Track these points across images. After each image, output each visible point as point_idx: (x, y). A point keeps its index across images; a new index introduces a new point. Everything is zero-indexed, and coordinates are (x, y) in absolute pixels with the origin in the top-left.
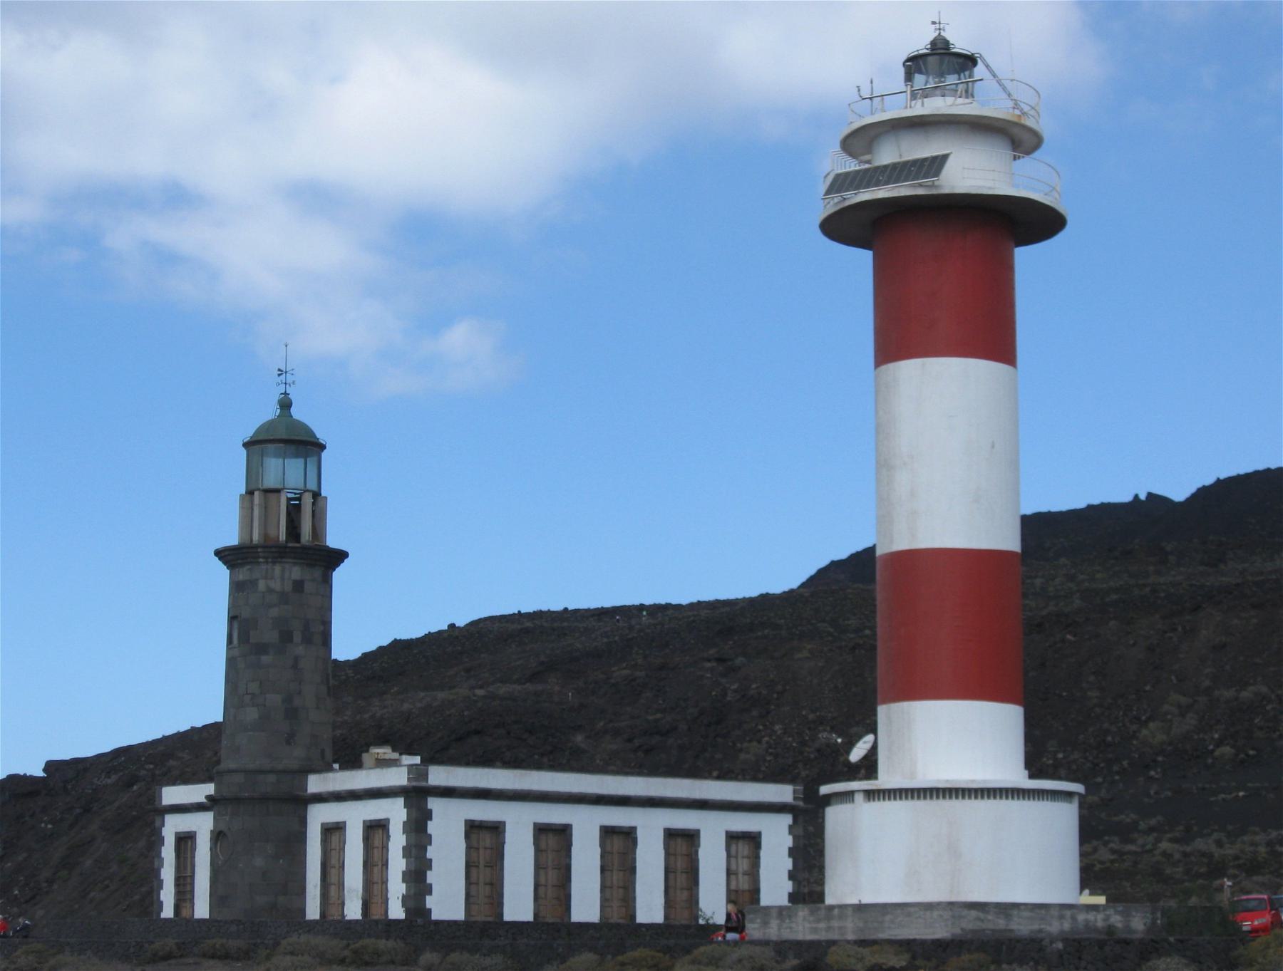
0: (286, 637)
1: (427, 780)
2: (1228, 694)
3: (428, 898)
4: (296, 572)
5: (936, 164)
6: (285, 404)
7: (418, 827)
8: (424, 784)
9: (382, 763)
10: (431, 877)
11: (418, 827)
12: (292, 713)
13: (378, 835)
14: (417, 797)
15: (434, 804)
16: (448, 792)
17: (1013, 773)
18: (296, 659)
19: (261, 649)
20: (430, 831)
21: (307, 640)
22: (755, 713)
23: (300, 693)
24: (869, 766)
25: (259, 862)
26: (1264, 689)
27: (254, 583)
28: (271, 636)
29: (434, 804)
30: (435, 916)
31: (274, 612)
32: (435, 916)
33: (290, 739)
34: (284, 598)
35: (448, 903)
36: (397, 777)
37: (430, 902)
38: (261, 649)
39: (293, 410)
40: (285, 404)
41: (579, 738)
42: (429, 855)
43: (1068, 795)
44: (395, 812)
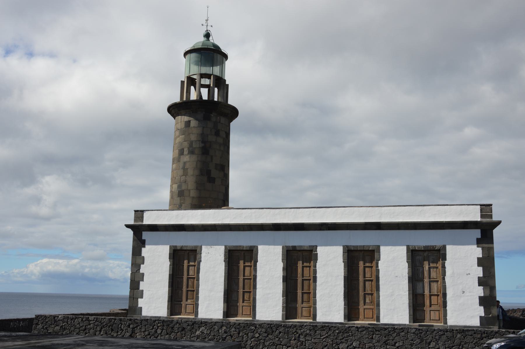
1: (142, 221)
3: (140, 300)
4: (186, 118)
6: (207, 35)
8: (140, 223)
10: (143, 286)
15: (145, 235)
18: (185, 163)
20: (143, 255)
21: (191, 152)
23: (185, 182)
29: (145, 235)
30: (145, 313)
32: (145, 313)
37: (141, 303)
39: (211, 38)
40: (207, 35)
42: (141, 271)
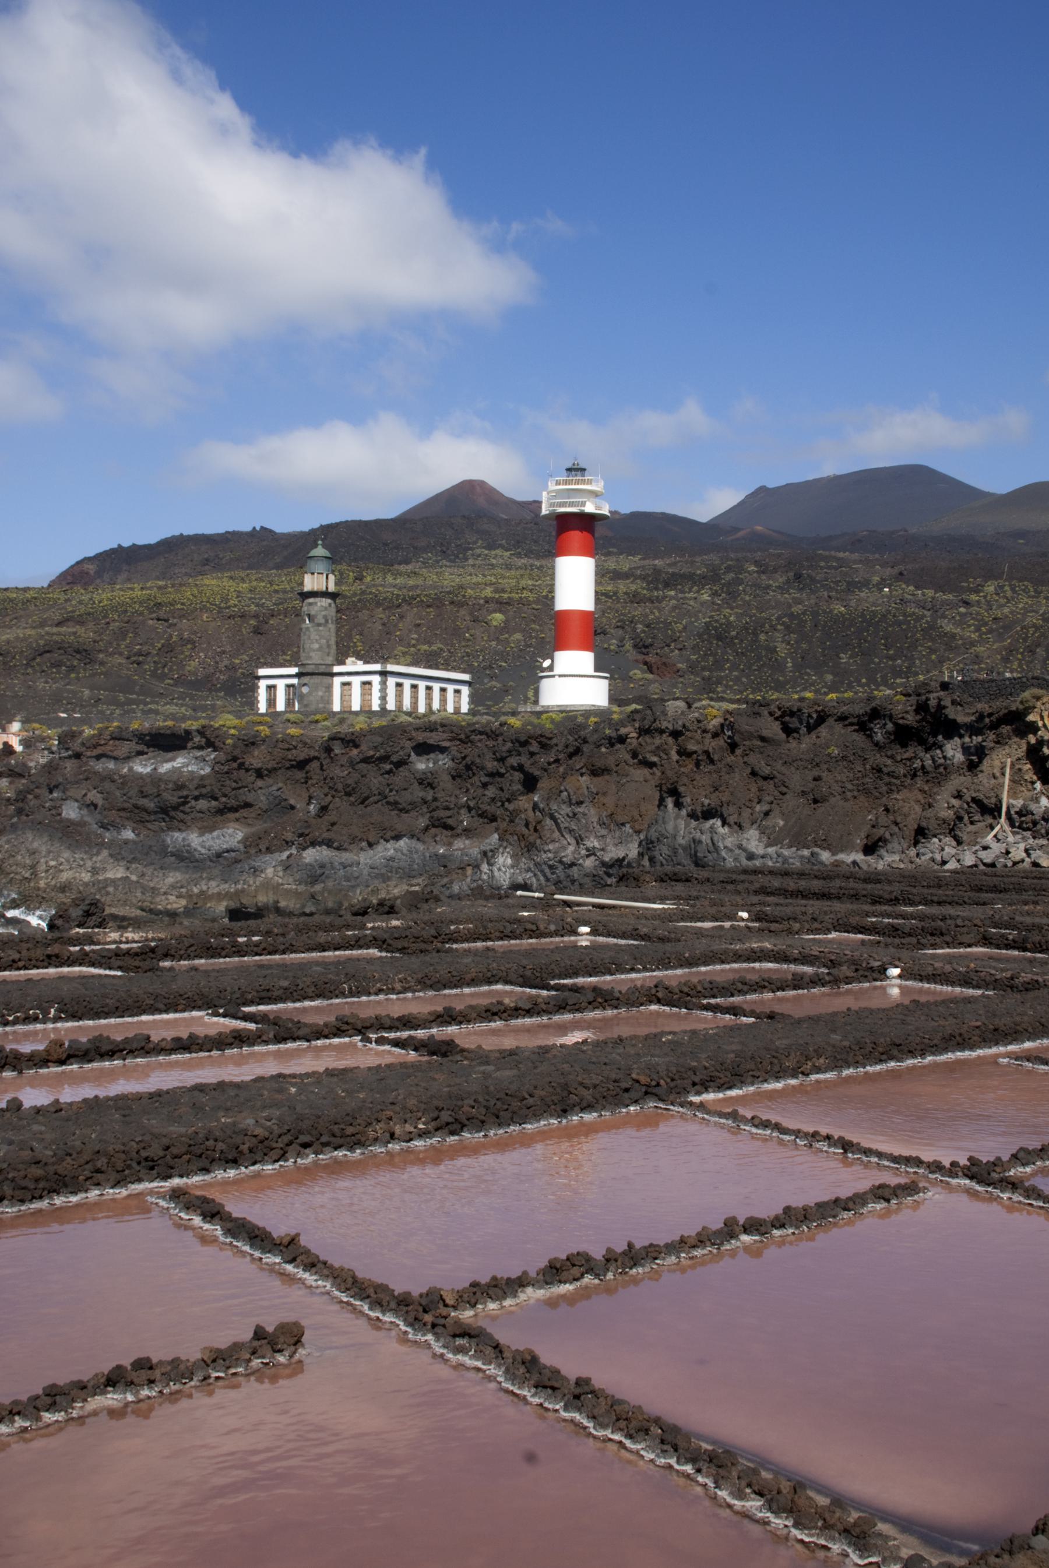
0: (327, 621)
2: (426, 647)
4: (329, 601)
5: (583, 504)
7: (384, 683)
9: (354, 663)
11: (384, 683)
12: (329, 646)
13: (346, 687)
14: (384, 674)
16: (393, 674)
17: (591, 671)
19: (319, 625)
22: (189, 646)
24: (551, 668)
25: (320, 693)
26: (441, 646)
27: (316, 603)
28: (322, 621)
31: (323, 613)
33: (328, 655)
34: (326, 609)
35: (376, 707)
36: (377, 667)
38: (319, 625)
41: (101, 656)
43: (606, 678)
44: (376, 679)
